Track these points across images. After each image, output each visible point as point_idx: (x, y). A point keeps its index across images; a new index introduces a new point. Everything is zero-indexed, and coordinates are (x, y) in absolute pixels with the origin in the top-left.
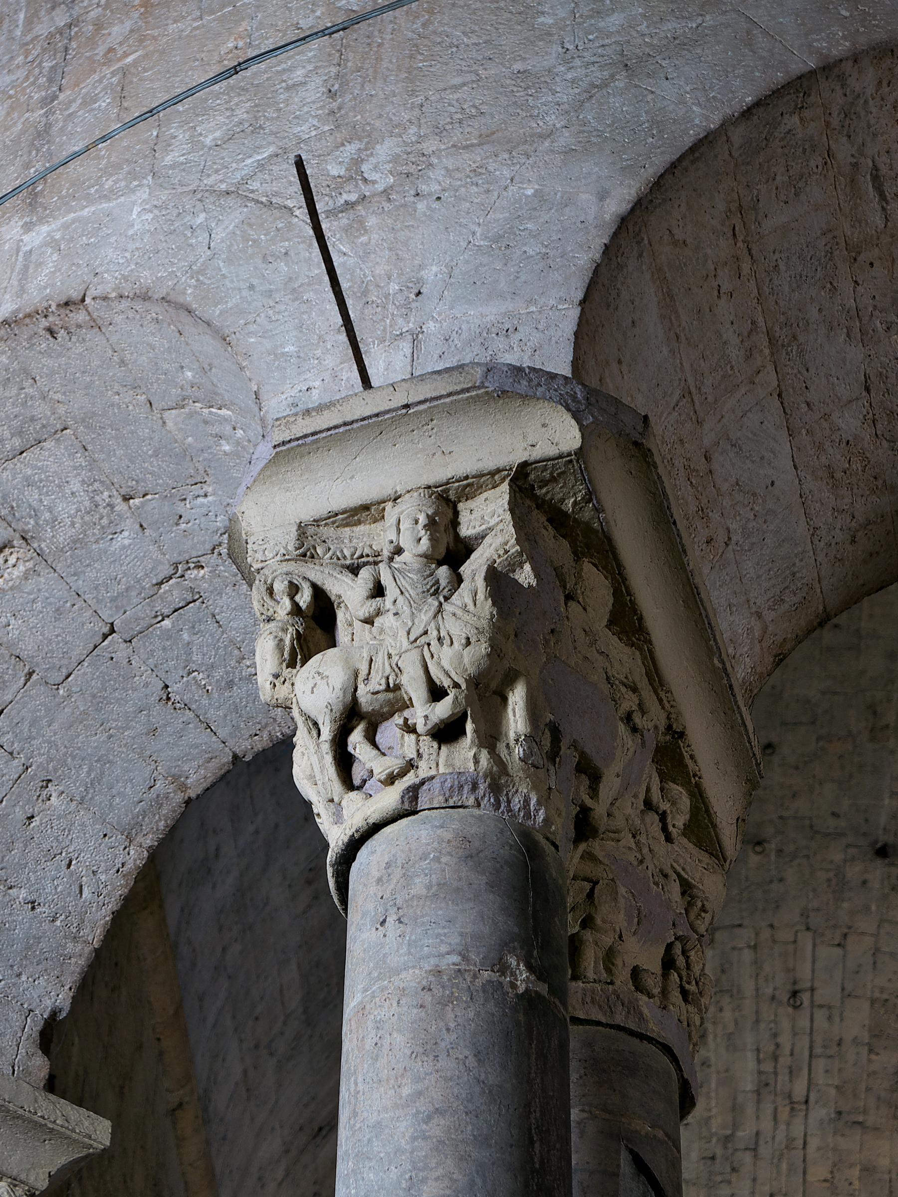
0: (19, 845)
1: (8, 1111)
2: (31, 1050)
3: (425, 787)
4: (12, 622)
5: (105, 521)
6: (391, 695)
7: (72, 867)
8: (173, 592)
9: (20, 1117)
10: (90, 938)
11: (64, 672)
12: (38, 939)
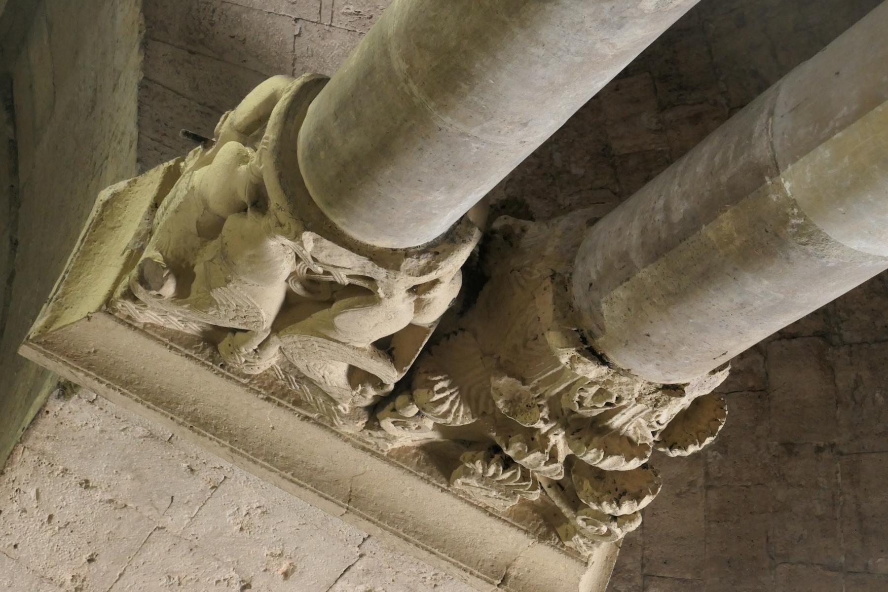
1: (138, 392)
7: (47, 516)
10: (27, 453)
12: (82, 456)
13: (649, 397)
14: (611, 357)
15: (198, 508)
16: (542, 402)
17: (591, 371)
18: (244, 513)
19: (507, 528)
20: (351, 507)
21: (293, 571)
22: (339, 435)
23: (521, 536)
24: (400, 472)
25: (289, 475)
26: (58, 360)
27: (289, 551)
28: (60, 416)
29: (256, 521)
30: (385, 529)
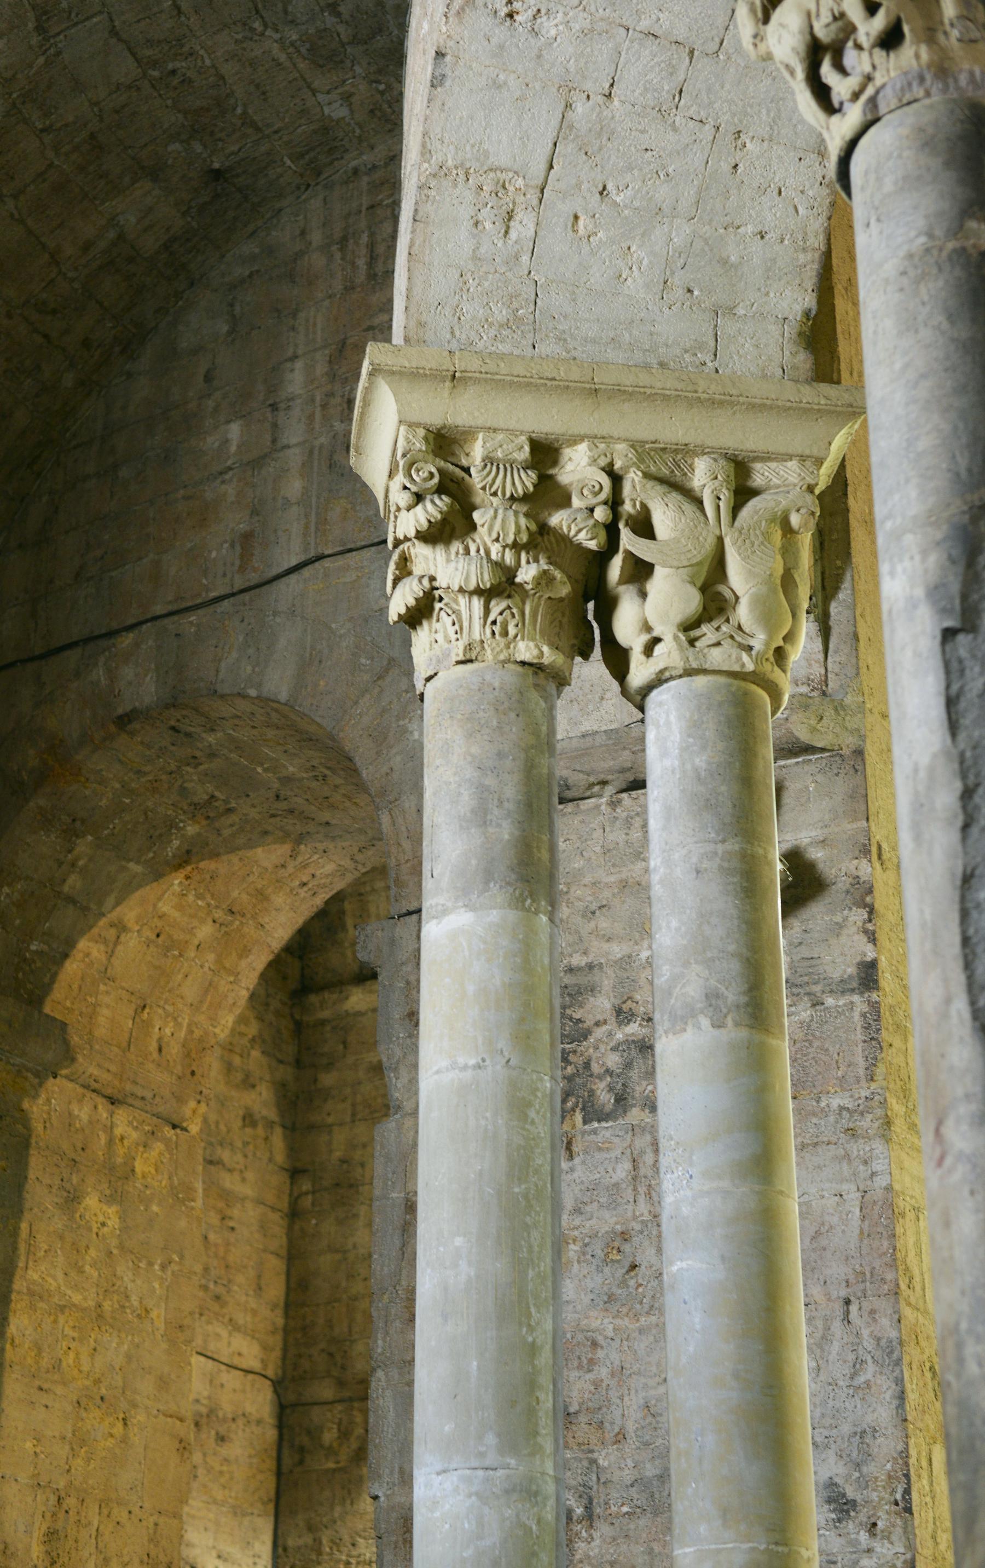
0: (734, 191)
1: (779, 407)
2: (794, 350)
3: (881, 95)
4: (661, 15)
6: (840, 23)
9: (790, 408)
10: (816, 245)
11: (717, 40)
12: (774, 260)
13: (478, 649)
14: (519, 669)
15: (670, 254)
16: (533, 592)
17: (525, 650)
18: (634, 268)
19: (473, 424)
20: (593, 386)
21: (573, 226)
22: (626, 440)
23: (459, 422)
24: (570, 432)
25: (648, 391)
26: (842, 406)
27: (586, 249)
28: (803, 291)
29: (620, 263)
30: (561, 380)
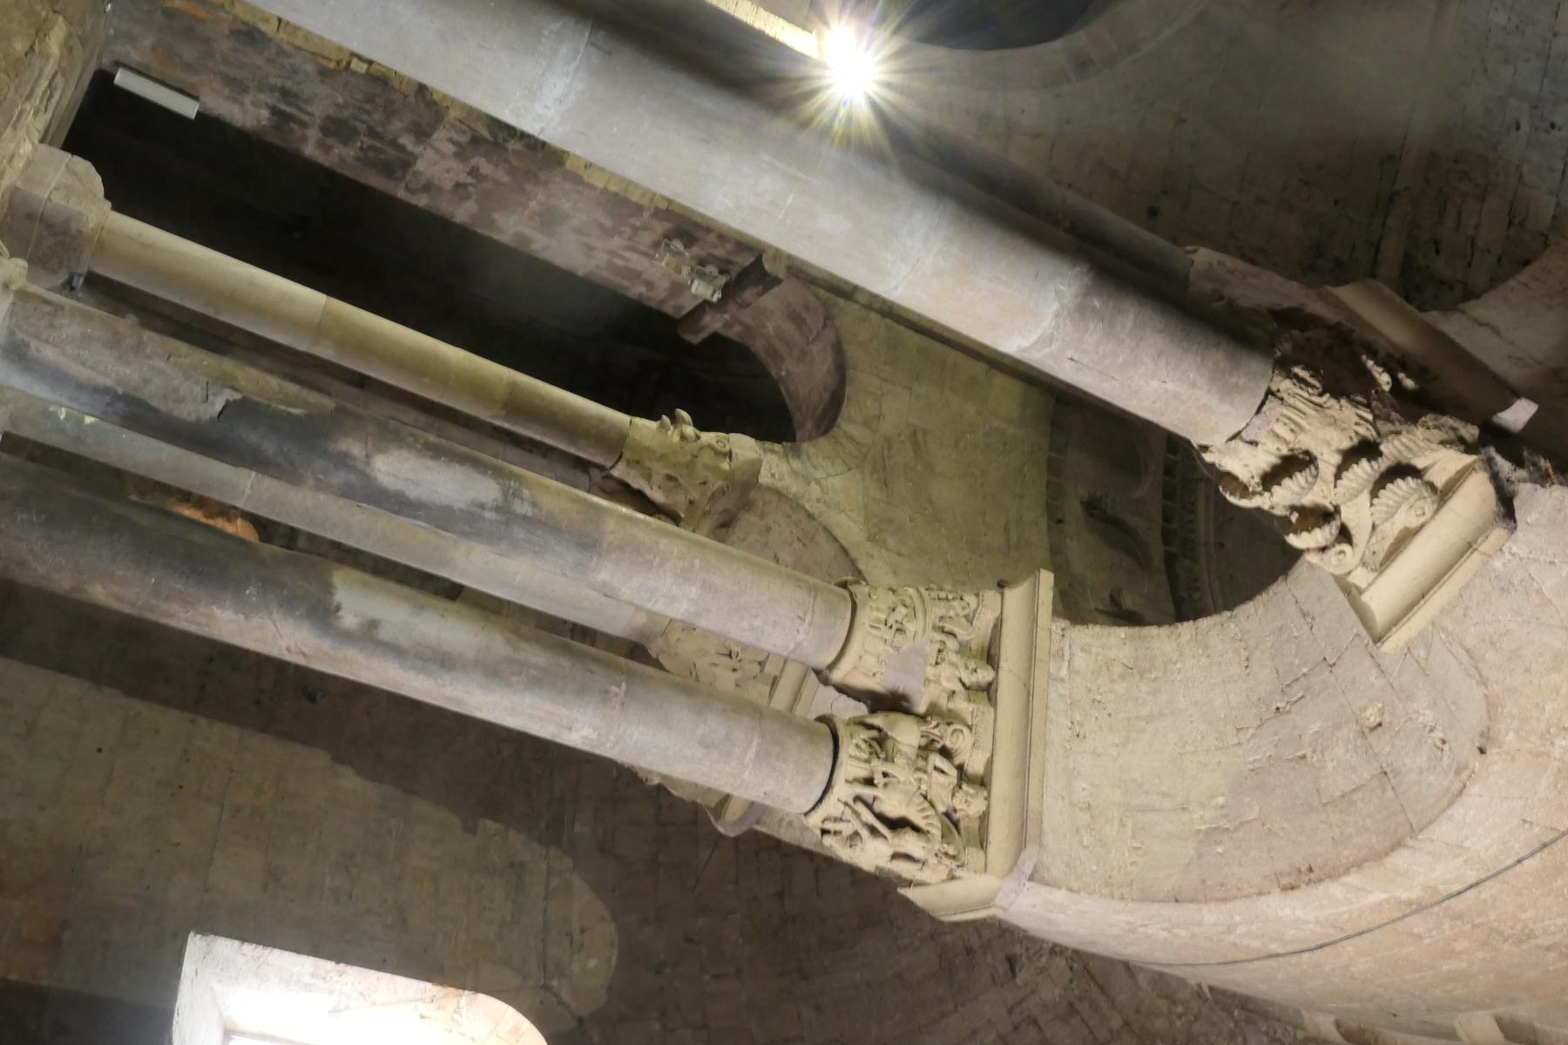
5: (1320, 741)
8: (1296, 692)
